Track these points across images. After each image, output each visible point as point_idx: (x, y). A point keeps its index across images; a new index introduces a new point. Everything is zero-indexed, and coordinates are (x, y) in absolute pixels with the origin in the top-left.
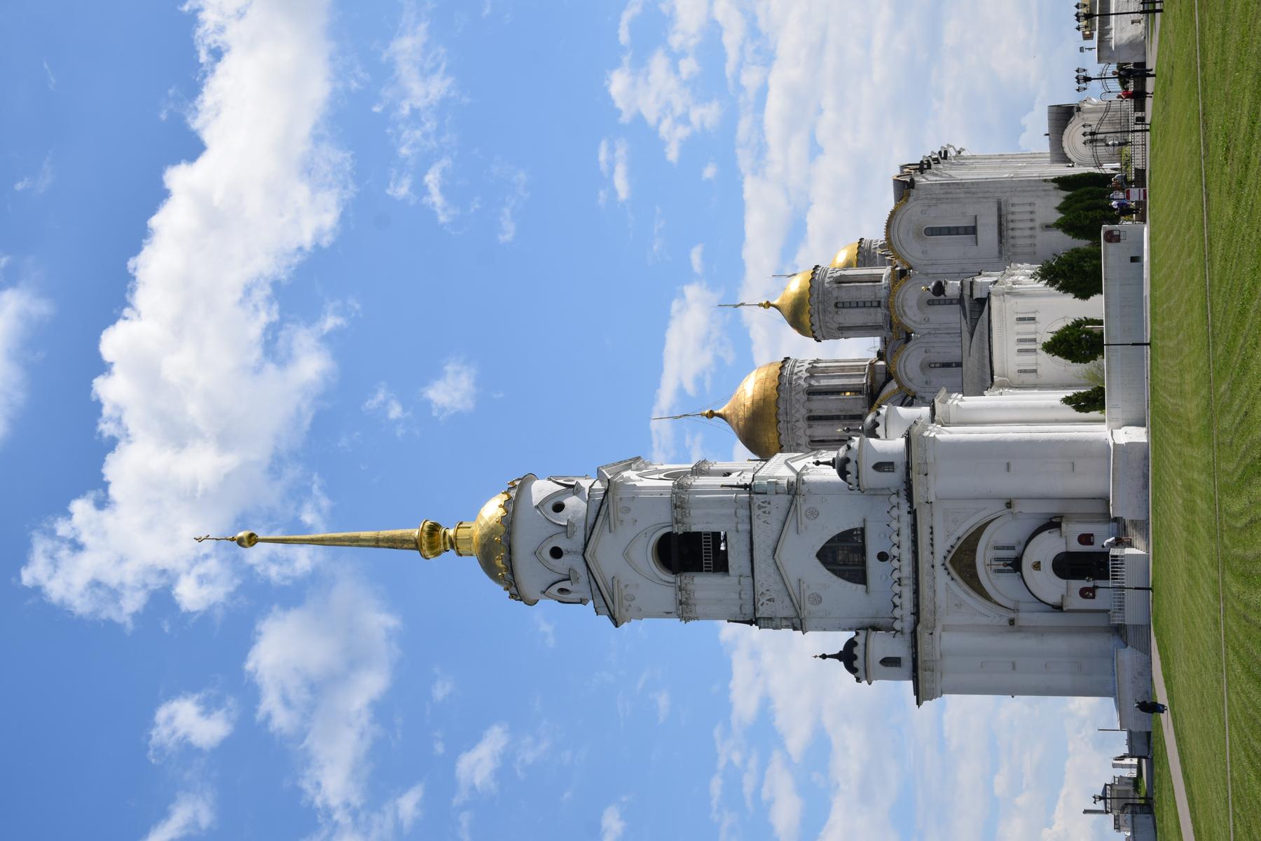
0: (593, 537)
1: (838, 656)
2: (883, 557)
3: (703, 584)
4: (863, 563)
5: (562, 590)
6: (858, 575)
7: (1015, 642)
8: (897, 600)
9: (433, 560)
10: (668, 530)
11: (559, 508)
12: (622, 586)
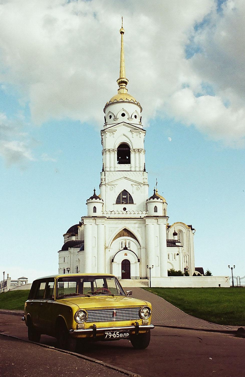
0: (128, 125)
1: (95, 194)
2: (125, 209)
3: (114, 156)
4: (122, 203)
5: (111, 117)
6: (119, 201)
7: (102, 247)
8: (113, 213)
9: (117, 83)
10: (131, 147)
11: (136, 117)
12: (114, 133)
